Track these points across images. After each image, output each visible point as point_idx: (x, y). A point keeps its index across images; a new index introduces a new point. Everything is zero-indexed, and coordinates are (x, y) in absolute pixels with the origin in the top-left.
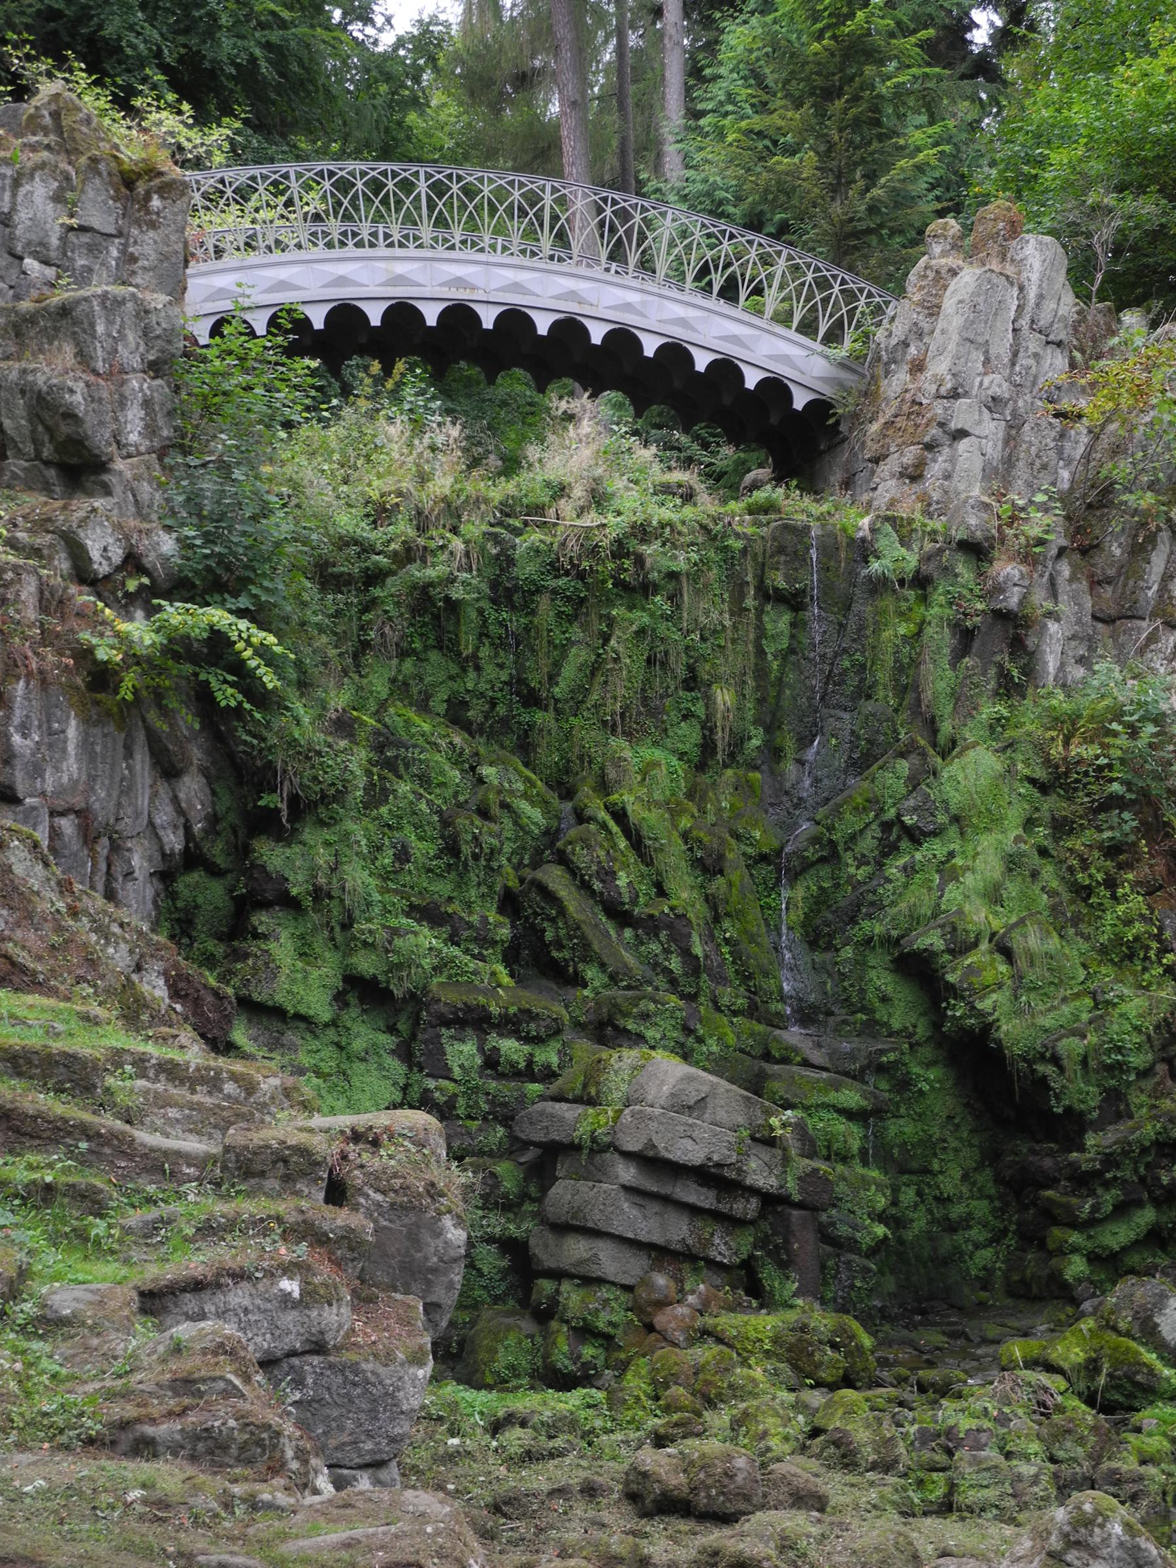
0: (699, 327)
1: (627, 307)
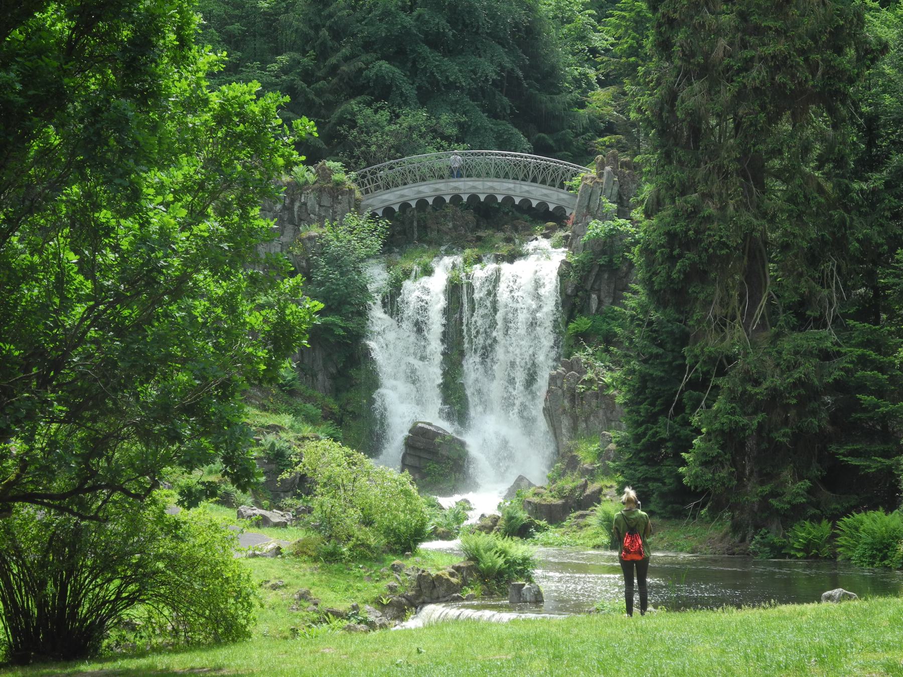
0: (534, 193)
1: (509, 189)
